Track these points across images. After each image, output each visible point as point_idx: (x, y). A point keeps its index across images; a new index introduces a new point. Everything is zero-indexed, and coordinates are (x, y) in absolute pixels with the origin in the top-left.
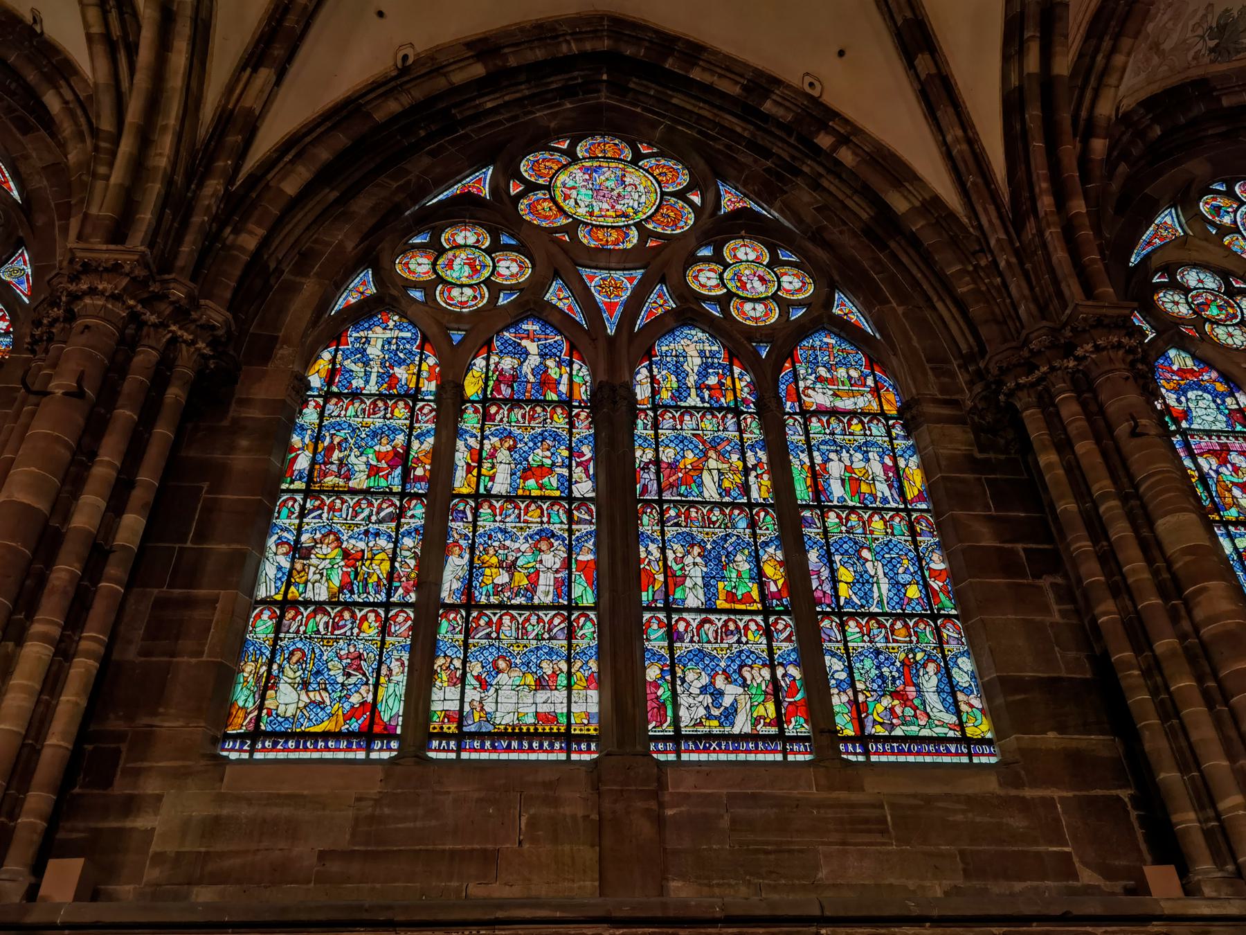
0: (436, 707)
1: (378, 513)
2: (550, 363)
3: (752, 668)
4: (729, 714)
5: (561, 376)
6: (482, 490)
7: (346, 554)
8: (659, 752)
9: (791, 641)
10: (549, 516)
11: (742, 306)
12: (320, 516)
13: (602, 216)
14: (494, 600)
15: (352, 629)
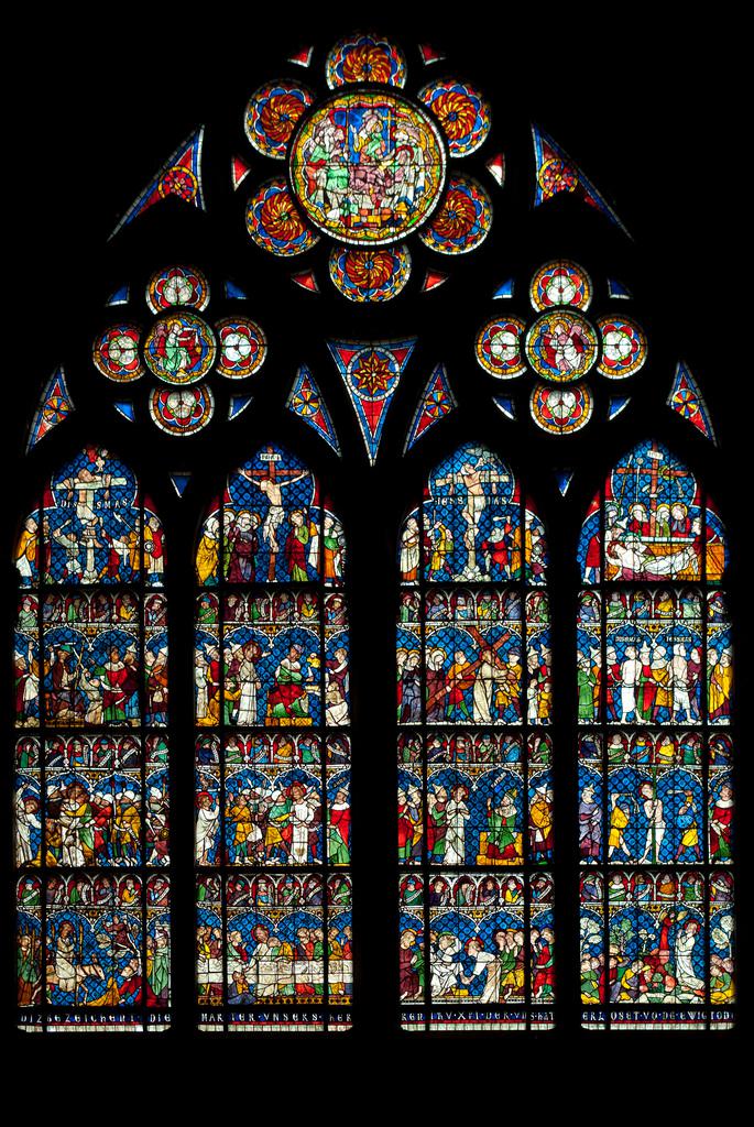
0: (202, 979)
2: (297, 519)
3: (506, 933)
4: (480, 982)
5: (310, 538)
6: (227, 721)
7: (95, 810)
8: (409, 1022)
10: (301, 755)
12: (60, 763)
15: (113, 898)
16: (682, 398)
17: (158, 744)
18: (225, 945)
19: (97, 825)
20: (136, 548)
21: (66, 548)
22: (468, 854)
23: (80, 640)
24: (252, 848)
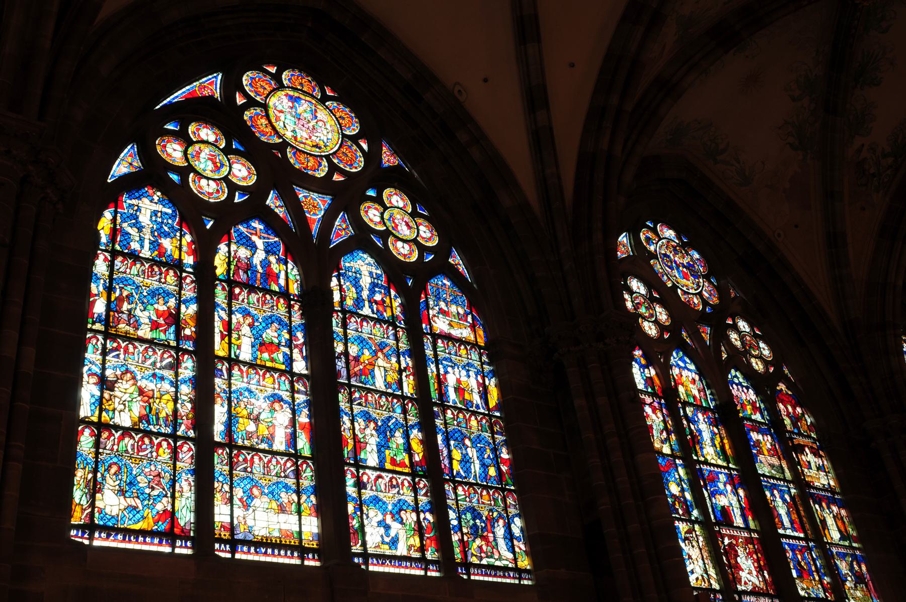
0: (217, 518)
1: (161, 361)
2: (272, 259)
3: (406, 512)
5: (280, 271)
6: (233, 356)
7: (141, 392)
9: (427, 496)
11: (396, 243)
12: (118, 356)
13: (303, 143)
14: (247, 443)
15: (151, 452)
16: (456, 260)
17: (187, 359)
21: (130, 234)
22: (381, 462)
24: (249, 435)
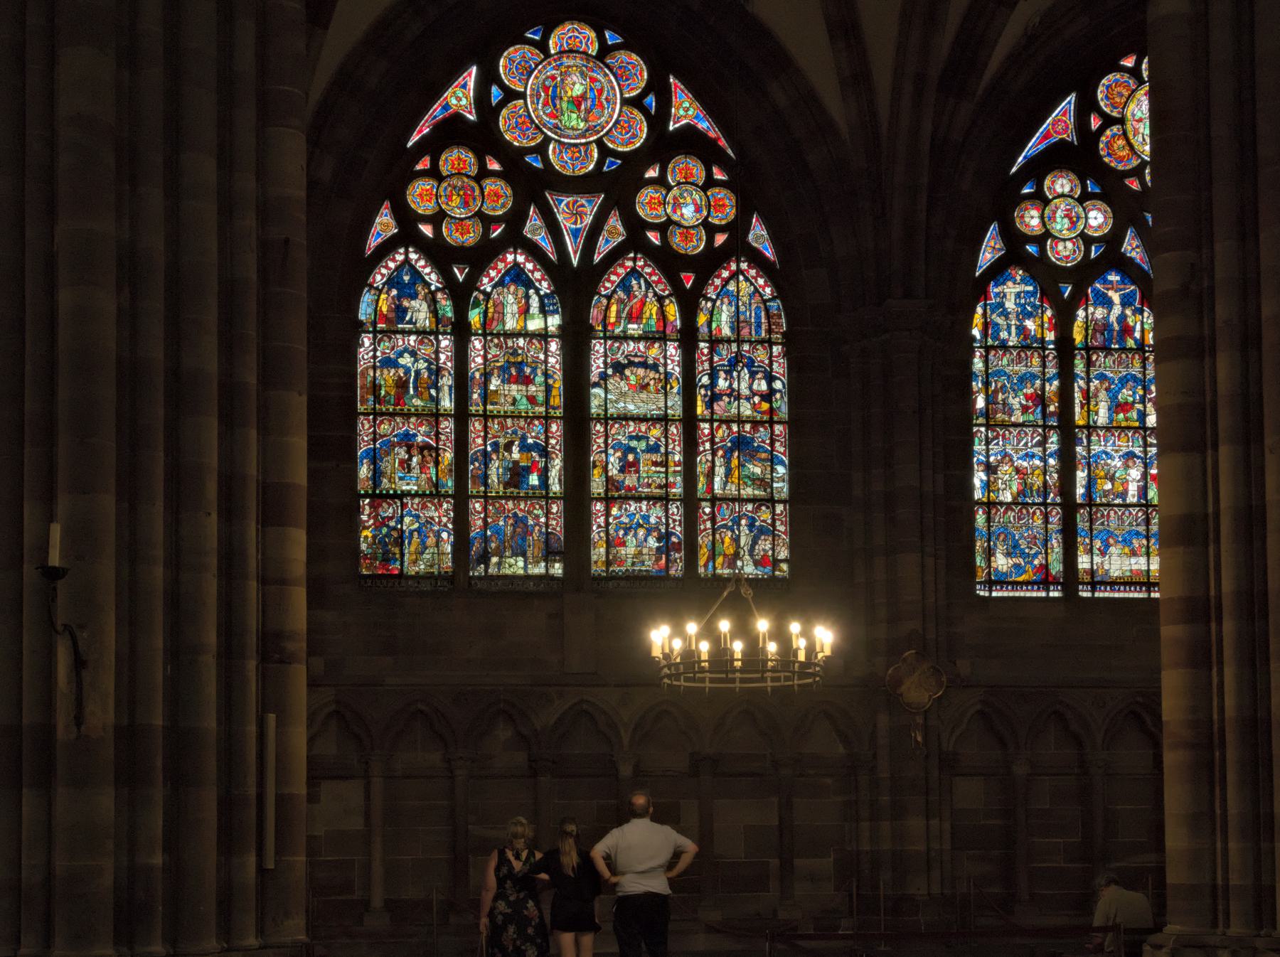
0: (1080, 566)
1: (1032, 441)
2: (1128, 312)
5: (1136, 323)
6: (1091, 423)
7: (1018, 470)
12: (997, 444)
15: (1028, 520)
18: (1092, 547)
19: (1018, 478)
20: (1039, 326)
23: (1009, 377)
24: (1106, 494)
